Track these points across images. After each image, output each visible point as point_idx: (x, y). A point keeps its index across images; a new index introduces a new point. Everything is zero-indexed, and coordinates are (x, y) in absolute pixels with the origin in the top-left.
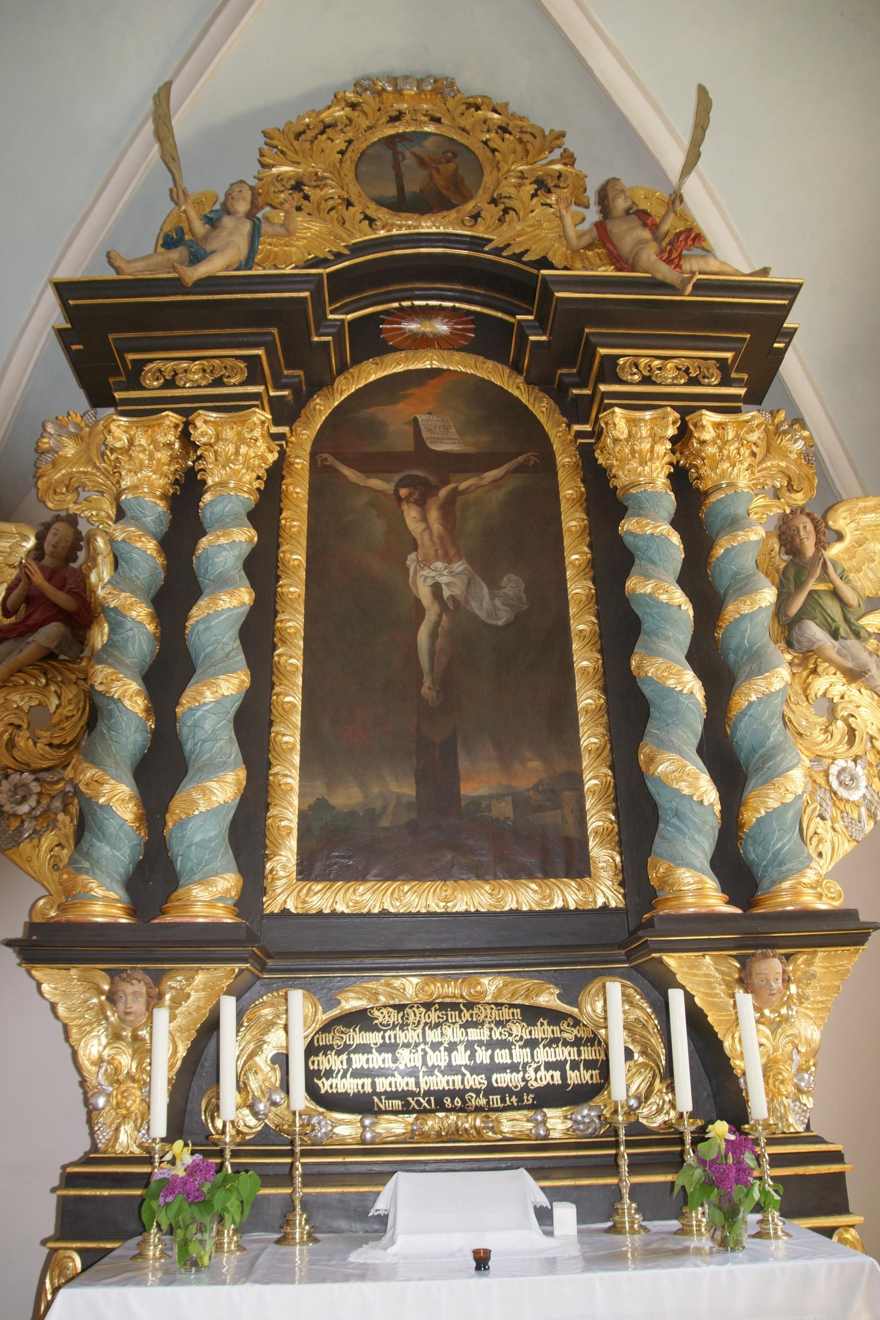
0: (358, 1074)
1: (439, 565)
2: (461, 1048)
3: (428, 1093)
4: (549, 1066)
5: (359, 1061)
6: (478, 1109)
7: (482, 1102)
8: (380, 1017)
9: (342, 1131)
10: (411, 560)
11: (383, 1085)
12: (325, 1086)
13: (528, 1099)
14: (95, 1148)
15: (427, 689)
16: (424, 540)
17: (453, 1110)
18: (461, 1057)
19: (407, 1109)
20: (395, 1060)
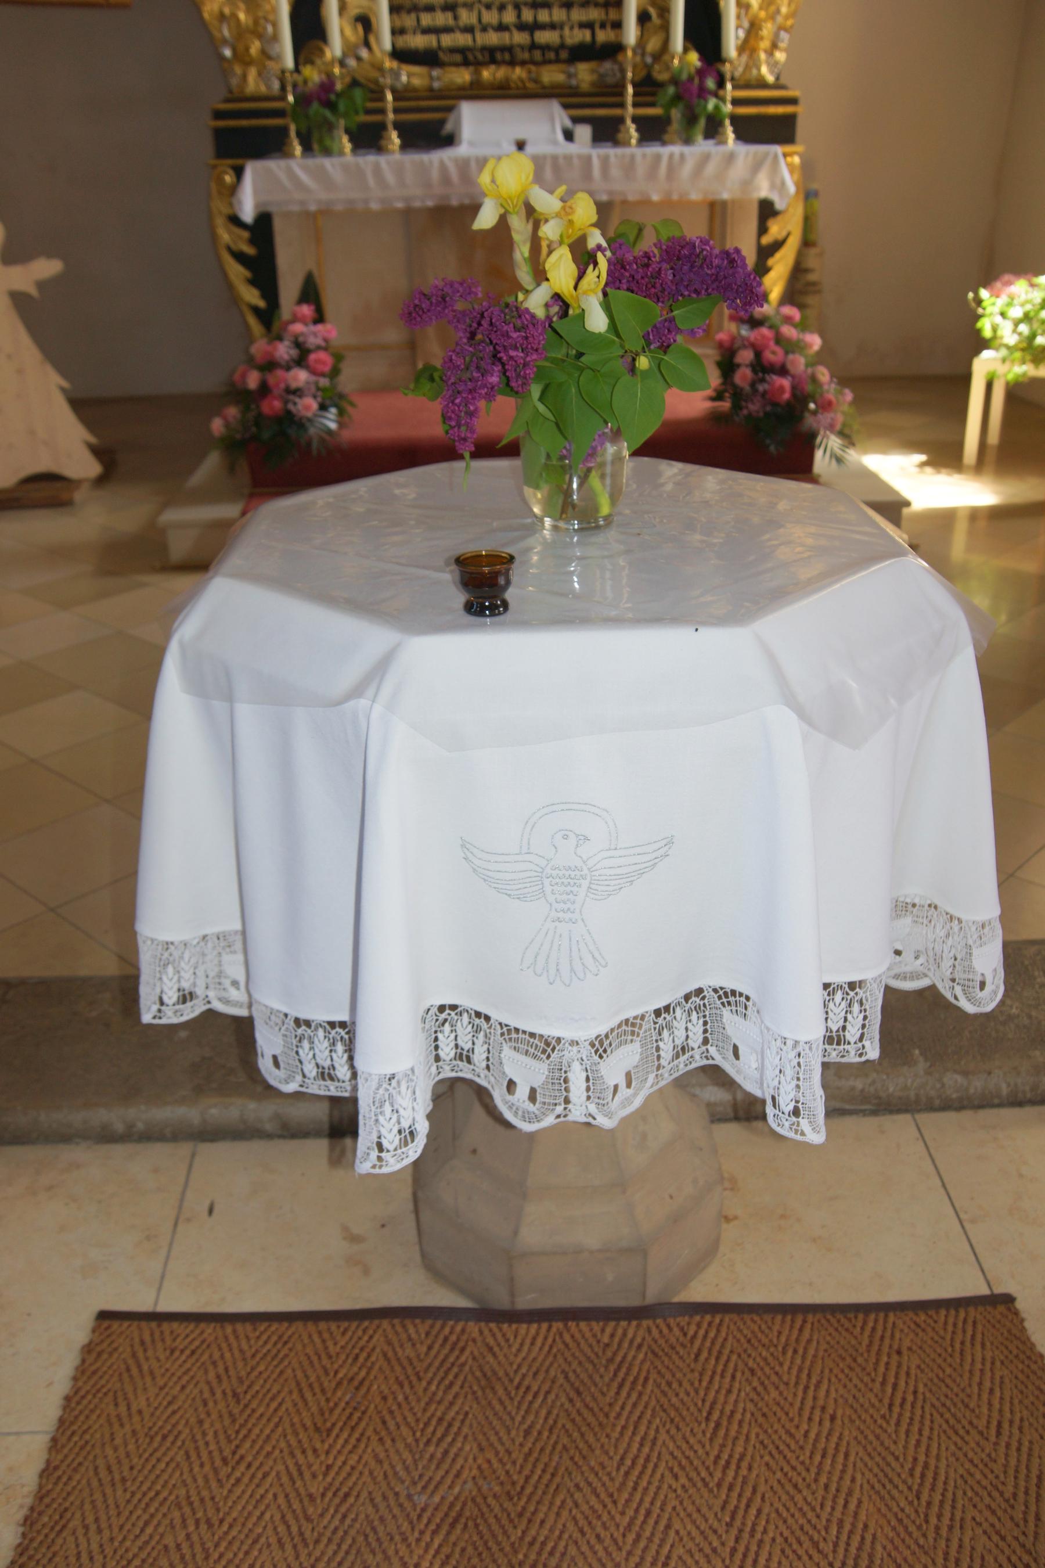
0: (427, 31)
2: (510, 8)
3: (484, 49)
4: (582, 25)
5: (426, 19)
6: (523, 63)
7: (526, 56)
9: (416, 82)
11: (447, 40)
13: (564, 55)
14: (231, 92)
17: (504, 62)
19: (466, 63)
20: (456, 18)
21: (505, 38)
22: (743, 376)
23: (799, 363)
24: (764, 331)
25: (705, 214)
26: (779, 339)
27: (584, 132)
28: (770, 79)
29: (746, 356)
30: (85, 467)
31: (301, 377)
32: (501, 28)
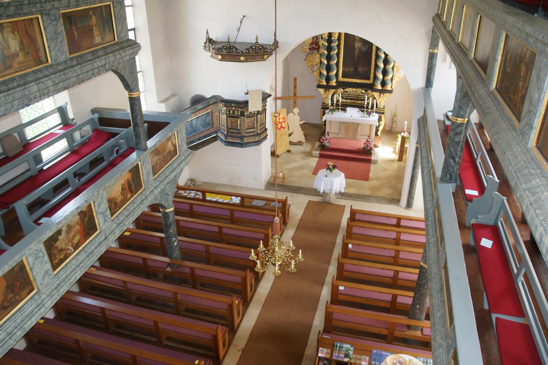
8: (348, 92)
11: (348, 97)
12: (343, 97)
15: (356, 58)
18: (355, 96)
21: (354, 98)
22: (366, 146)
25: (369, 126)
26: (369, 143)
27: (360, 112)
28: (382, 108)
30: (304, 141)
31: (326, 142)
32: (354, 97)
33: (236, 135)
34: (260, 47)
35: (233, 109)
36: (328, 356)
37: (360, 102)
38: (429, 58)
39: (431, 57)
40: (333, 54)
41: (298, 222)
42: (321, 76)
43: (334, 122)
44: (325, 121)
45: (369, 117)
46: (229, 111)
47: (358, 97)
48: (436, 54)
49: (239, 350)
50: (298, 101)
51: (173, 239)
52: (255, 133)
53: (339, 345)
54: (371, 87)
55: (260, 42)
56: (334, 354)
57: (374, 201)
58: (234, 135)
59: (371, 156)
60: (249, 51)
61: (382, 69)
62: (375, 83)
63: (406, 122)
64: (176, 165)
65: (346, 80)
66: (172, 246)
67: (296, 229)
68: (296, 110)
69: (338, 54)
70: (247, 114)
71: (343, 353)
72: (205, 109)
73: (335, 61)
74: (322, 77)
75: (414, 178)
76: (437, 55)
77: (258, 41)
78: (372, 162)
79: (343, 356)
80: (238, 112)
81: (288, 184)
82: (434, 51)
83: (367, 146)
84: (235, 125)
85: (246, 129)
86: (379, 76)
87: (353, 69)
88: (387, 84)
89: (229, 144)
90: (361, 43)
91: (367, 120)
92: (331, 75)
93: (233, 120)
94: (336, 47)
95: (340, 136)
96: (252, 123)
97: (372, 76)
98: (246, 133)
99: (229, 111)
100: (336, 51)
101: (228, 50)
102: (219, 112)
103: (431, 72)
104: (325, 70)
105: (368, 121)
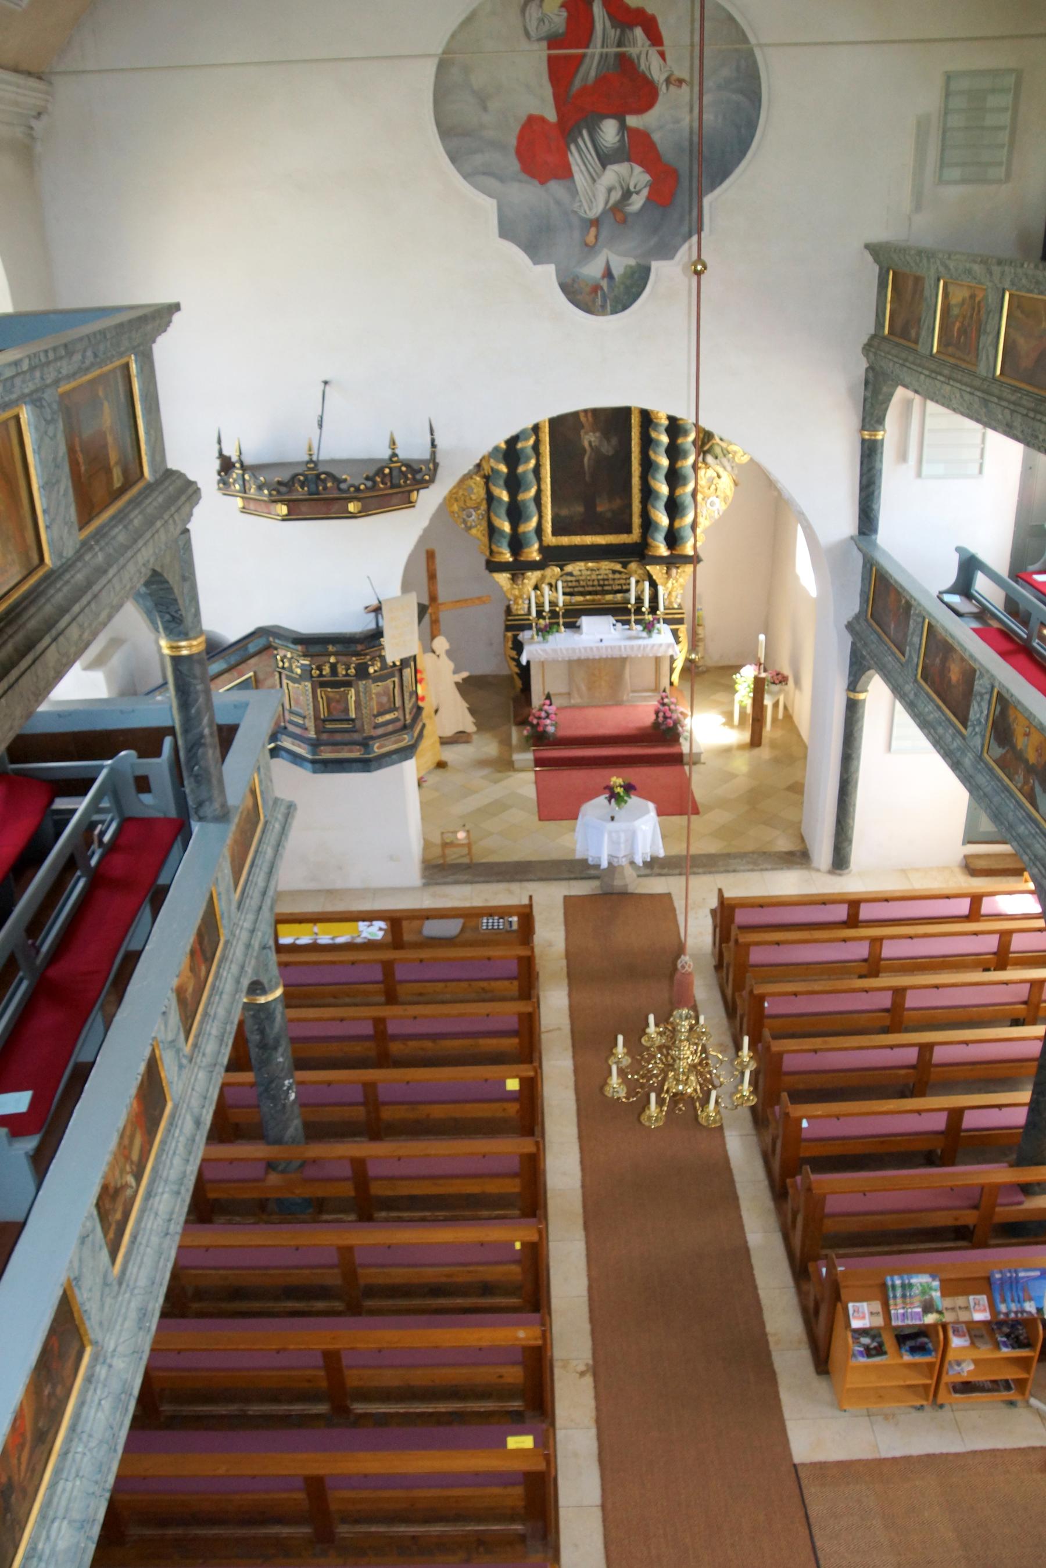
0: (570, 587)
1: (591, 434)
10: (582, 433)
11: (576, 590)
15: (587, 478)
16: (586, 425)
18: (596, 583)
21: (594, 589)
22: (661, 720)
23: (675, 716)
24: (667, 707)
26: (670, 709)
27: (619, 625)
28: (676, 606)
29: (661, 715)
31: (548, 722)
32: (593, 586)
33: (346, 737)
34: (404, 469)
35: (332, 660)
36: (879, 1321)
37: (609, 597)
38: (862, 456)
39: (867, 452)
40: (525, 473)
41: (564, 962)
42: (496, 536)
43: (555, 661)
44: (528, 662)
45: (650, 636)
46: (320, 668)
47: (604, 585)
48: (879, 444)
49: (582, 1374)
50: (444, 616)
51: (287, 1082)
52: (399, 725)
53: (898, 1282)
54: (640, 552)
55: (403, 454)
56: (893, 1312)
57: (742, 868)
58: (338, 737)
59: (680, 744)
60: (375, 483)
61: (665, 499)
62: (650, 540)
63: (762, 637)
64: (270, 852)
65: (565, 540)
66: (284, 1106)
67: (570, 985)
68: (441, 644)
69: (537, 470)
70: (375, 671)
71: (917, 1301)
72: (235, 673)
73: (533, 492)
74: (499, 541)
75: (850, 788)
76: (882, 445)
77: (397, 451)
78: (686, 759)
79: (919, 1310)
80: (348, 668)
81: (484, 860)
82: (875, 435)
83: (665, 718)
84: (342, 706)
85: (376, 716)
86: (659, 521)
87: (580, 509)
88: (682, 538)
89: (326, 767)
90: (598, 434)
91: (645, 647)
92: (524, 533)
93: (331, 695)
94: (530, 452)
95: (576, 700)
96: (389, 695)
97: (636, 521)
98: (376, 726)
99: (320, 668)
100: (532, 463)
101: (313, 487)
102: (280, 673)
103: (873, 493)
104: (506, 518)
105: (648, 649)
